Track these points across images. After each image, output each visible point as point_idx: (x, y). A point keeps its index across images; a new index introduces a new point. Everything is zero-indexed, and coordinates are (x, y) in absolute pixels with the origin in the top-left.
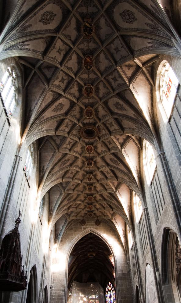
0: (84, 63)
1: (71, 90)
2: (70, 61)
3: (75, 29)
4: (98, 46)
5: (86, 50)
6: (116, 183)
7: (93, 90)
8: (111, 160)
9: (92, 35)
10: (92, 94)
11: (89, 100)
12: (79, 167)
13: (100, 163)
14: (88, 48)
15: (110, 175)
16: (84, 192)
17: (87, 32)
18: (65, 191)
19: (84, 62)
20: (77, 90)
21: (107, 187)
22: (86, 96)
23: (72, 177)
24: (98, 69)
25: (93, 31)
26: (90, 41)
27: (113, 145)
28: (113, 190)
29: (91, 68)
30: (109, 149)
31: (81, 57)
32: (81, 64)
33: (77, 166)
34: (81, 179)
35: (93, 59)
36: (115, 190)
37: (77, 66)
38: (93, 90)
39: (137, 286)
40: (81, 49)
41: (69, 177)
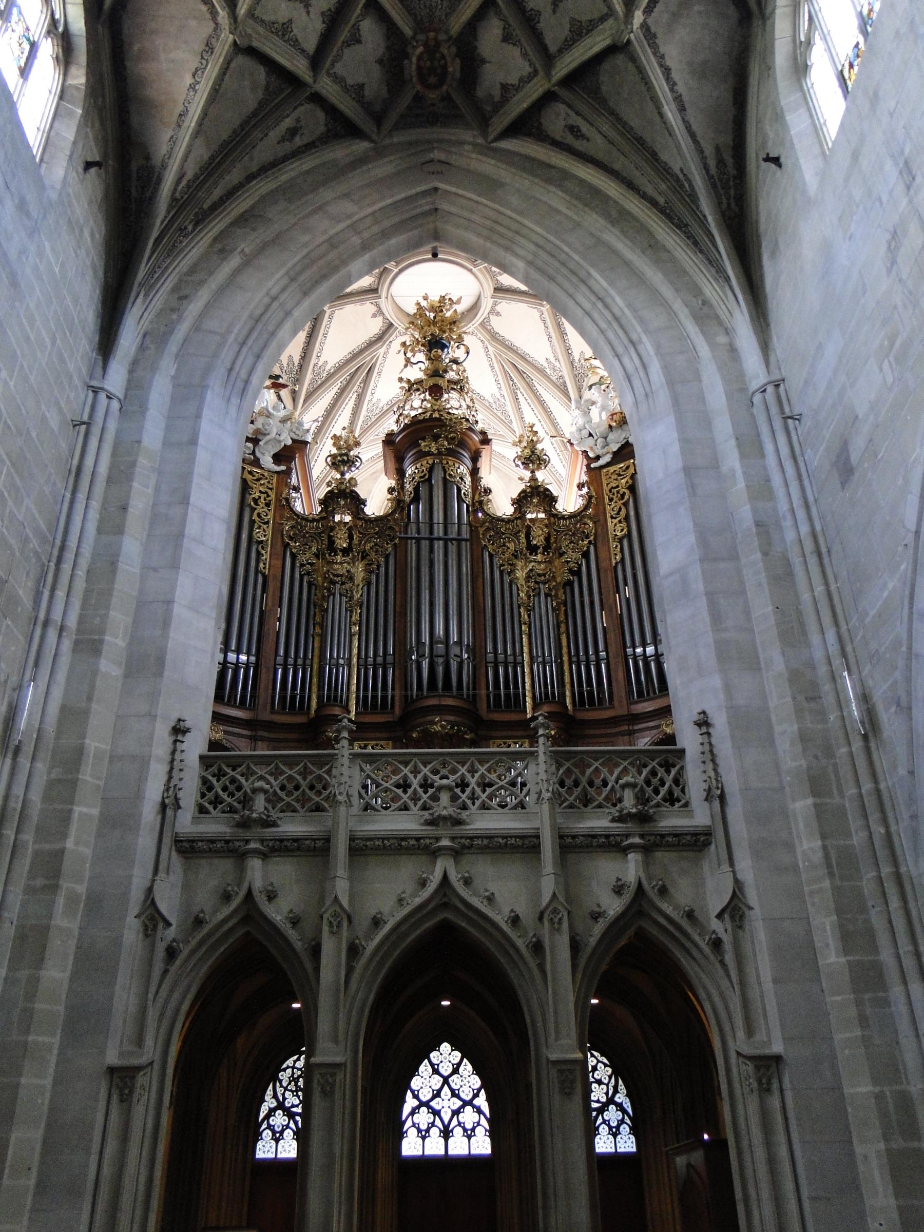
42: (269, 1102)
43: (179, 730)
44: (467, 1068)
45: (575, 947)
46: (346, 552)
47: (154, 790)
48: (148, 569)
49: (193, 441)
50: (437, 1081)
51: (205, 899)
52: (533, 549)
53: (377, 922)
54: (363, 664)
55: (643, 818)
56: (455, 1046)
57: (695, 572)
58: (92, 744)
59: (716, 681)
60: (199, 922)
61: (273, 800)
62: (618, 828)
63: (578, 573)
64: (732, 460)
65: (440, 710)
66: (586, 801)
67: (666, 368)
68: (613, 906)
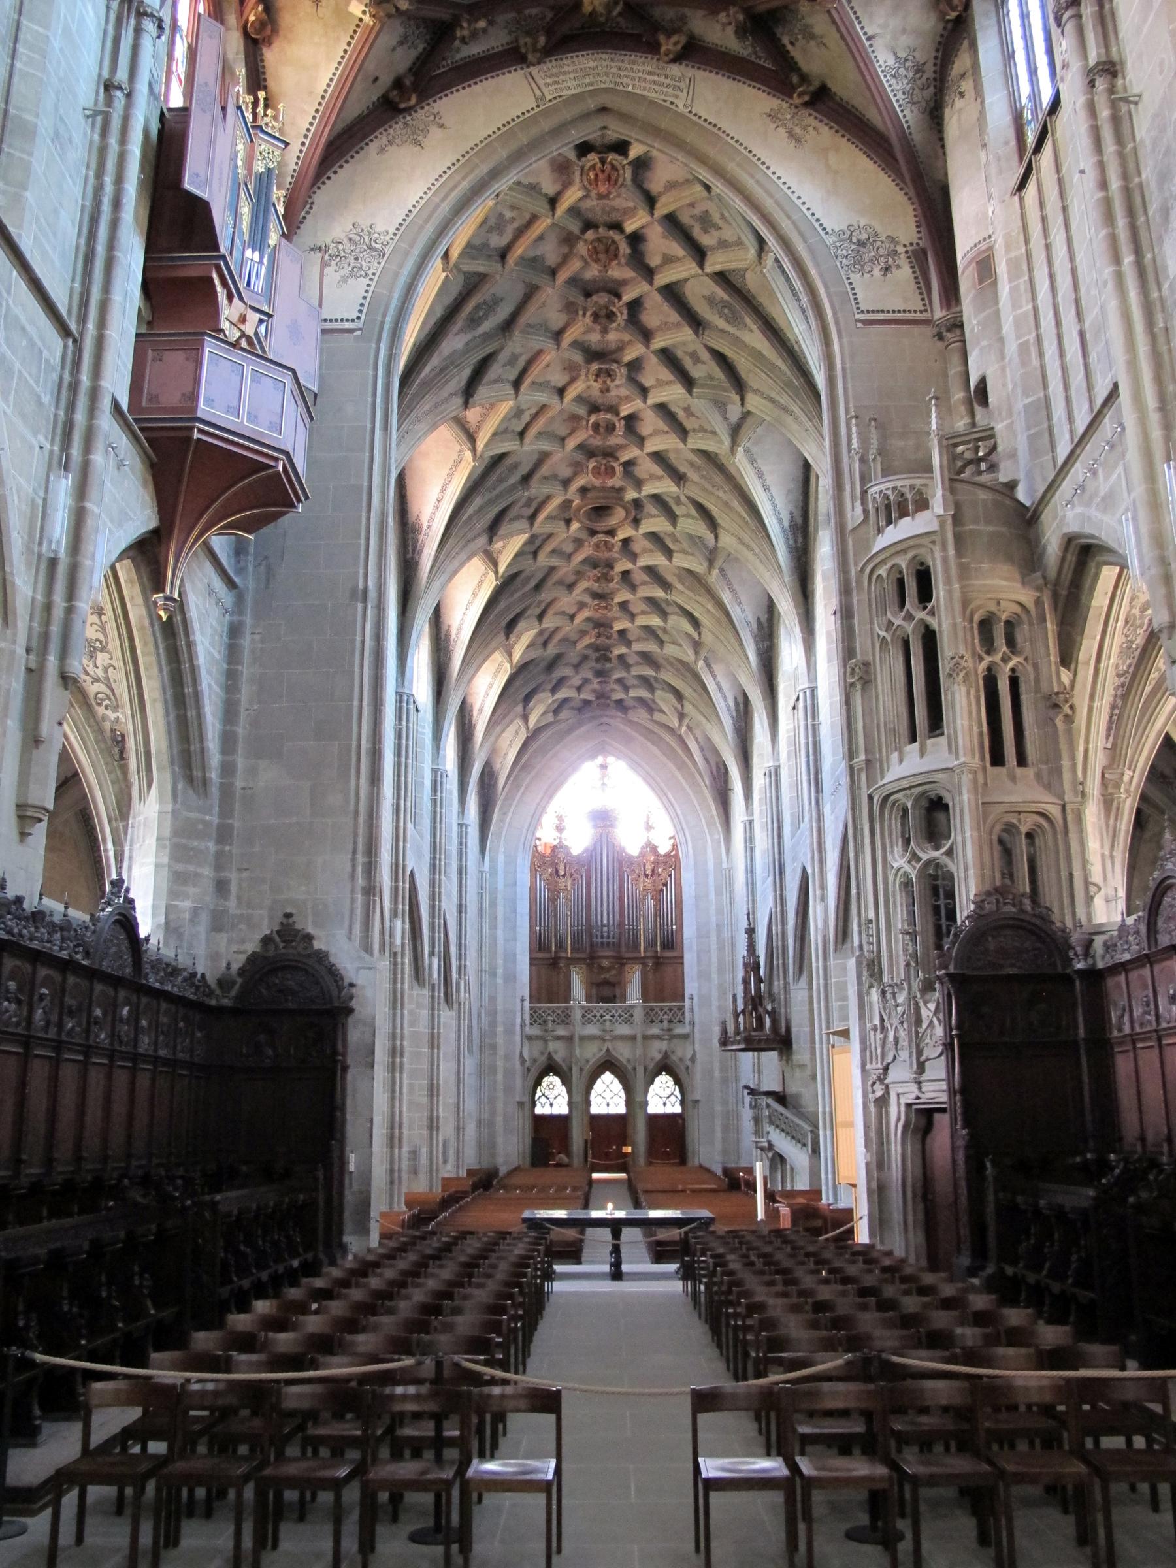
6: (734, 412)
8: (711, 301)
12: (547, 329)
13: (657, 313)
15: (704, 370)
16: (571, 444)
18: (480, 445)
21: (689, 424)
23: (513, 376)
27: (728, 234)
28: (721, 442)
30: (699, 253)
33: (541, 327)
34: (560, 385)
36: (727, 442)
39: (804, 870)
41: (496, 381)
42: (538, 1094)
43: (522, 1000)
44: (616, 1081)
45: (645, 1069)
46: (564, 876)
47: (518, 1021)
48: (506, 941)
49: (515, 884)
50: (604, 1087)
51: (536, 1054)
52: (646, 876)
53: (587, 1061)
54: (573, 933)
55: (669, 1030)
56: (612, 1073)
57: (695, 941)
58: (499, 1008)
59: (696, 984)
60: (535, 1061)
61: (554, 1021)
62: (661, 1033)
63: (666, 885)
64: (712, 896)
65: (606, 957)
66: (652, 1022)
67: (694, 847)
68: (658, 1057)
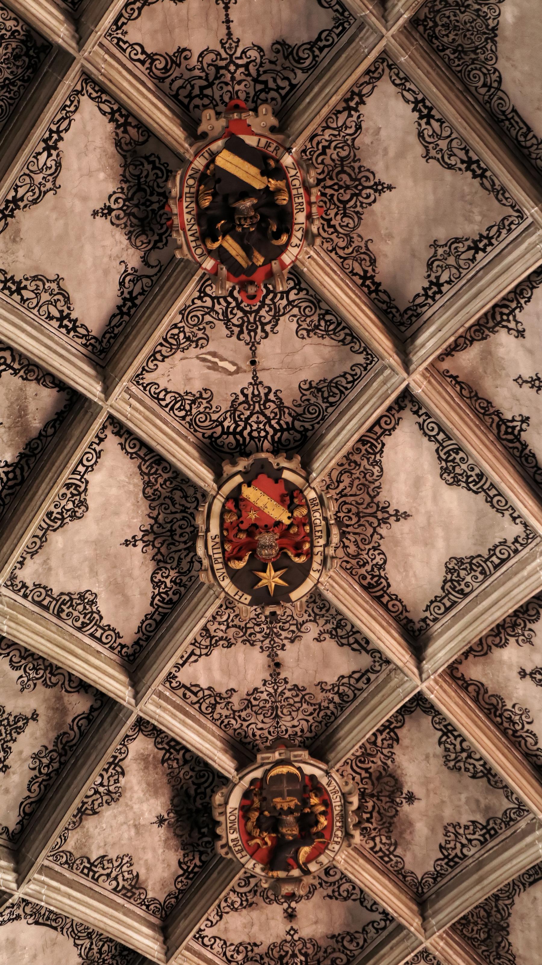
0: (224, 540)
1: (90, 823)
2: (72, 526)
3: (107, 211)
4: (360, 359)
5: (233, 409)
7: (327, 803)
9: (287, 258)
10: (326, 846)
11: (291, 916)
14: (256, 382)
17: (240, 239)
19: (215, 530)
20: (161, 821)
22: (258, 870)
24: (367, 588)
25: (300, 218)
26: (266, 315)
29: (294, 586)
31: (187, 480)
32: (193, 548)
35: (311, 495)
37: (151, 566)
38: (336, 802)
40: (179, 398)
